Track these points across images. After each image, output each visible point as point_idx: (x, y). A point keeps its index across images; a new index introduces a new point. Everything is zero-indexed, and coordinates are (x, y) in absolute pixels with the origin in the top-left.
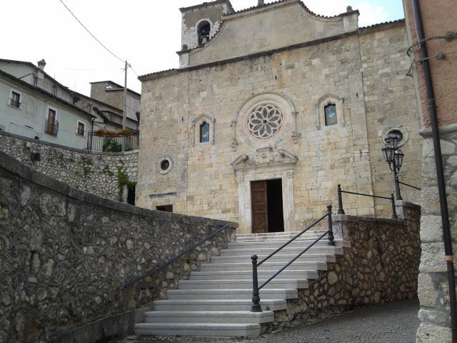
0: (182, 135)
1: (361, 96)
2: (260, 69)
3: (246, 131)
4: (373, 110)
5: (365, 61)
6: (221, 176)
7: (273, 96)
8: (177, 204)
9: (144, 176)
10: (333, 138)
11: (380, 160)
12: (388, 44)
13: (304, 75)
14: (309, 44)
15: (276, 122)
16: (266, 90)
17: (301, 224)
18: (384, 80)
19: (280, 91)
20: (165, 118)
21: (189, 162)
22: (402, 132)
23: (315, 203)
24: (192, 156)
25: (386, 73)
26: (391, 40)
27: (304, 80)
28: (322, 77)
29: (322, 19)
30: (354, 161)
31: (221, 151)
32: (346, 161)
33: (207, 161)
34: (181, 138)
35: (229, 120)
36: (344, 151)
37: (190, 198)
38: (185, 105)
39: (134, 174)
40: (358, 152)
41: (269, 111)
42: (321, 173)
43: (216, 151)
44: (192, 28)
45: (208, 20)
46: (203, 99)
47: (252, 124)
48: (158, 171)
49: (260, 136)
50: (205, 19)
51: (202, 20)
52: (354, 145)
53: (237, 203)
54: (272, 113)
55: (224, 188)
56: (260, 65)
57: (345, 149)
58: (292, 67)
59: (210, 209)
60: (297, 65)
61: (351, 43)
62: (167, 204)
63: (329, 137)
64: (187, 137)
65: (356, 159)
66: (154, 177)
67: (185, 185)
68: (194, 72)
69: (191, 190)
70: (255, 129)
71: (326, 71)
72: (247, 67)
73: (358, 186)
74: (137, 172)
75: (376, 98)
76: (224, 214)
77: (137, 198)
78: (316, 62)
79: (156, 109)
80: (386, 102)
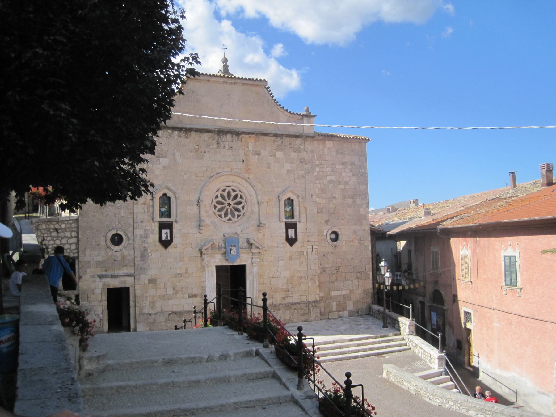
1: (314, 197)
2: (227, 147)
4: (322, 212)
5: (318, 166)
7: (239, 180)
9: (88, 250)
11: (324, 256)
12: (335, 154)
13: (269, 165)
14: (276, 135)
15: (240, 207)
18: (330, 186)
19: (246, 176)
22: (340, 233)
25: (332, 181)
26: (337, 151)
29: (285, 112)
32: (301, 254)
35: (194, 198)
37: (152, 281)
39: (73, 247)
40: (311, 247)
42: (281, 263)
46: (164, 167)
48: (108, 247)
52: (308, 241)
54: (236, 197)
55: (190, 271)
56: (227, 143)
58: (259, 154)
59: (176, 293)
61: (309, 146)
62: (123, 286)
64: (146, 210)
65: (309, 253)
66: (103, 253)
69: (152, 272)
70: (219, 210)
71: (288, 166)
72: (214, 142)
73: (309, 277)
74: (77, 244)
75: (324, 201)
76: (191, 299)
78: (279, 154)
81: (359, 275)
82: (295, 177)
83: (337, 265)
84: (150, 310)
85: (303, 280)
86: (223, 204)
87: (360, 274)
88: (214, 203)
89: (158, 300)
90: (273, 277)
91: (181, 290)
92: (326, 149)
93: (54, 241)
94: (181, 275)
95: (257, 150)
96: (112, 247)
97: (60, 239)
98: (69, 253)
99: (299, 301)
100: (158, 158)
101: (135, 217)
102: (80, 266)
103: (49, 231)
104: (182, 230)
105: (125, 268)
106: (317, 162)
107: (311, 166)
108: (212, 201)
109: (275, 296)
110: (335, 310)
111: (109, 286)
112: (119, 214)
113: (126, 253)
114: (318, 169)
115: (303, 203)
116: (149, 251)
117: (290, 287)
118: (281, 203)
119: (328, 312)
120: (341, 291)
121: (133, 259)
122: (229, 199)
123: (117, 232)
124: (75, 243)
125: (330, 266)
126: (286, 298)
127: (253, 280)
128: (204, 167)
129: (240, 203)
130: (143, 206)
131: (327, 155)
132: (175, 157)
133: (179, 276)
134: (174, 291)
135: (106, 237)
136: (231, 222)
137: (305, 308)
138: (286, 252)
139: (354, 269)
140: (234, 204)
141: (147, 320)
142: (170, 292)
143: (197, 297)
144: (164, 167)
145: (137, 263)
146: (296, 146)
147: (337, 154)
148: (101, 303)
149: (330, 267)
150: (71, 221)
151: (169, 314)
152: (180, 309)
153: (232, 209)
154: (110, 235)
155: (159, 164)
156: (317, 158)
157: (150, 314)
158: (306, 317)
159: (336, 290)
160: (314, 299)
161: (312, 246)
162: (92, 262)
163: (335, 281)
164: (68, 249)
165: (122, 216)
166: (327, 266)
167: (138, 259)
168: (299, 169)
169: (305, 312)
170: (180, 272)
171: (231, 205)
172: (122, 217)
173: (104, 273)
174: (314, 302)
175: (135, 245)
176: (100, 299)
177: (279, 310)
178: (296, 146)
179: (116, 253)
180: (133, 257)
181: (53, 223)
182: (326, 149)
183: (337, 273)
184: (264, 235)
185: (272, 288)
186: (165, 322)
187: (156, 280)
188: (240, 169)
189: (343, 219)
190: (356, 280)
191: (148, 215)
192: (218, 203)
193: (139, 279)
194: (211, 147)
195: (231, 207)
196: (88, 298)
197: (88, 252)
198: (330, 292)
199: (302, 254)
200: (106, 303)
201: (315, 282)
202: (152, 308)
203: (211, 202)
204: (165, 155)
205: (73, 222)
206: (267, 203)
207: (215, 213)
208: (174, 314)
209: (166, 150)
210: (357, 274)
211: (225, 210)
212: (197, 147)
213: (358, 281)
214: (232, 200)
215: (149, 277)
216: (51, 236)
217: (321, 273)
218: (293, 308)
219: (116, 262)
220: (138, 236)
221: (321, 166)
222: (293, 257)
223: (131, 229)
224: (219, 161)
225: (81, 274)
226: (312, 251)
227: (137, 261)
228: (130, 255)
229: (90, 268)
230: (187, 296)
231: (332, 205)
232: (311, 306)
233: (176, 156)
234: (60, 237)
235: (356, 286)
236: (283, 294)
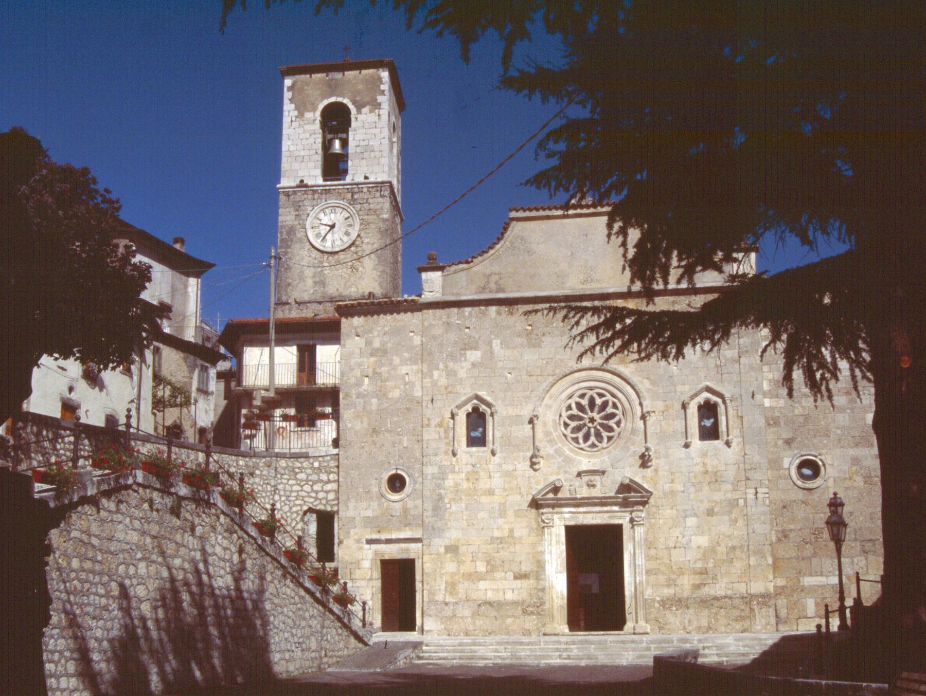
0: (432, 429)
1: (758, 397)
6: (510, 513)
8: (426, 558)
9: (353, 500)
10: (711, 463)
11: (784, 507)
17: (657, 605)
20: (396, 394)
21: (449, 482)
23: (681, 572)
24: (453, 472)
30: (746, 505)
32: (733, 504)
33: (484, 484)
34: (430, 434)
36: (729, 487)
37: (452, 549)
38: (436, 374)
39: (331, 496)
40: (753, 491)
41: (599, 401)
42: (691, 521)
43: (500, 465)
44: (309, 115)
45: (346, 101)
47: (568, 421)
49: (582, 445)
50: (340, 99)
51: (333, 99)
52: (747, 479)
53: (540, 565)
55: (517, 534)
57: (733, 484)
59: (492, 571)
62: (404, 556)
64: (443, 435)
65: (750, 502)
66: (375, 504)
67: (440, 524)
68: (455, 310)
69: (453, 535)
73: (751, 547)
76: (518, 582)
77: (341, 542)
79: (375, 373)
80: (796, 412)
81: (868, 546)
83: (816, 526)
84: (447, 597)
85: (738, 552)
86: (581, 418)
87: (870, 544)
89: (461, 580)
90: (675, 547)
91: (501, 565)
93: (302, 486)
94: (501, 540)
96: (389, 496)
97: (310, 483)
98: (325, 505)
99: (729, 592)
100: (463, 352)
101: (425, 446)
102: (340, 525)
103: (293, 471)
104: (504, 466)
105: (407, 528)
107: (750, 340)
108: (560, 416)
109: (678, 582)
110: (813, 615)
111: (383, 556)
112: (400, 443)
113: (410, 504)
115: (735, 408)
116: (446, 501)
117: (711, 565)
118: (688, 411)
119: (797, 617)
120: (827, 576)
121: (421, 513)
122: (592, 411)
124: (335, 491)
125: (799, 528)
126: (702, 586)
127: (635, 553)
128: (542, 359)
129: (612, 416)
130: (438, 429)
132: (491, 347)
133: (499, 541)
134: (489, 567)
136: (595, 449)
137: (743, 607)
139: (855, 534)
141: (441, 612)
142: (481, 567)
143: (529, 578)
144: (474, 365)
145: (427, 521)
148: (371, 584)
149: (800, 530)
150: (329, 458)
151: (479, 605)
152: (499, 597)
153: (598, 427)
154: (386, 476)
155: (465, 360)
157: (446, 604)
158: (746, 624)
159: (813, 574)
160: (763, 590)
161: (756, 489)
162: (358, 519)
163: (810, 558)
164: (323, 498)
165: (405, 445)
166: (792, 527)
167: (428, 513)
169: (743, 614)
170: (500, 535)
171: (595, 421)
173: (375, 536)
174: (763, 596)
175: (424, 491)
176: (368, 577)
177: (688, 608)
179: (394, 504)
180: (421, 510)
181: (299, 460)
183: (816, 541)
185: (674, 568)
186: (473, 616)
189: (828, 436)
190: (861, 555)
191: (446, 443)
192: (572, 417)
193: (430, 545)
194: (554, 325)
196: (351, 574)
197: (351, 505)
198: (801, 579)
199: (735, 503)
201: (764, 557)
202: (451, 593)
203: (558, 417)
204: (474, 345)
205: (332, 459)
206: (661, 413)
207: (565, 436)
208: (488, 606)
209: (477, 336)
210: (864, 544)
211: (585, 430)
212: (530, 328)
213: (866, 559)
214: (599, 413)
215: (447, 542)
216: (296, 479)
217: (779, 540)
218: (716, 605)
219: (394, 518)
220: (429, 477)
222: (716, 510)
223: (418, 466)
225: (341, 537)
226: (757, 498)
227: (427, 517)
228: (416, 507)
229: (355, 528)
230: (510, 575)
231: (801, 410)
232: (755, 603)
233: (494, 345)
234: (310, 480)
235: (862, 568)
236: (697, 580)
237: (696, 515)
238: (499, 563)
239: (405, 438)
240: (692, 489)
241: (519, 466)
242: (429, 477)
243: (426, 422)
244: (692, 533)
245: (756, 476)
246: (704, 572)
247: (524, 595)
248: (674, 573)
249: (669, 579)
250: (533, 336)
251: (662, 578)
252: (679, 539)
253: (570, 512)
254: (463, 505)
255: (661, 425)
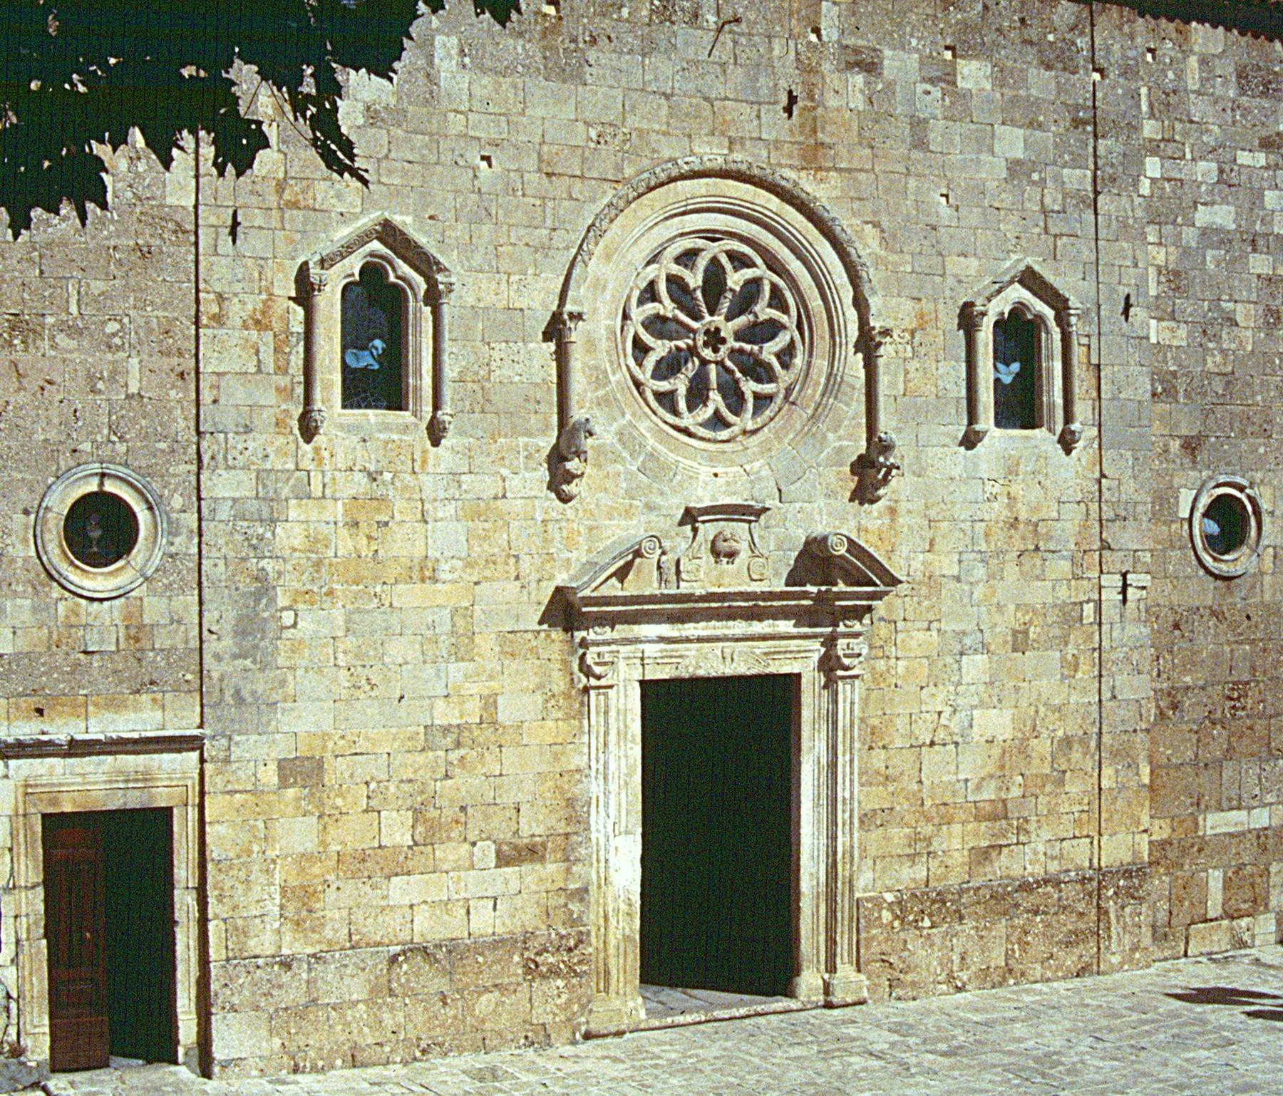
0: (232, 335)
3: (619, 378)
5: (1154, 148)
6: (486, 643)
10: (1027, 495)
11: (1176, 626)
13: (919, 125)
16: (740, 158)
17: (886, 916)
21: (289, 536)
25: (1219, 230)
27: (917, 154)
28: (992, 170)
31: (486, 485)
32: (1070, 616)
36: (1066, 565)
42: (975, 666)
52: (1105, 546)
55: (505, 715)
58: (871, 67)
60: (891, 60)
62: (134, 801)
63: (1016, 489)
64: (269, 363)
65: (1110, 612)
82: (1048, 201)
85: (1076, 755)
88: (636, 327)
89: (331, 877)
90: (932, 744)
92: (1193, 61)
94: (457, 735)
95: (860, 43)
96: (74, 576)
99: (1054, 867)
101: (206, 397)
106: (1150, 129)
108: (626, 316)
111: (54, 802)
113: (154, 609)
114: (1153, 167)
116: (282, 601)
117: (1016, 792)
120: (1250, 809)
121: (195, 644)
123: (101, 484)
125: (1201, 683)
126: (994, 854)
128: (588, 124)
130: (254, 334)
131: (1198, 93)
133: (449, 740)
135: (38, 512)
136: (724, 434)
137: (1081, 907)
138: (1000, 608)
140: (739, 336)
143: (542, 859)
146: (1051, 37)
147: (1242, 91)
151: (393, 960)
152: (452, 927)
154: (61, 501)
156: (1151, 106)
157: (287, 965)
159: (1225, 804)
161: (1124, 575)
165: (133, 389)
168: (1066, 157)
171: (723, 341)
172: (129, 397)
174: (1128, 874)
177: (961, 918)
178: (1051, 37)
182: (1193, 61)
184: (892, 511)
185: (928, 803)
187: (320, 764)
188: (777, 144)
193: (227, 761)
195: (723, 350)
200: (37, 901)
201: (1133, 765)
207: (638, 384)
211: (691, 368)
215: (284, 748)
217: (1162, 714)
220: (225, 512)
221: (1170, 149)
224: (667, 97)
226: (1124, 601)
227: (218, 658)
230: (487, 851)
232: (1111, 892)
233: (439, 53)
237: (985, 648)
238: (450, 813)
239: (134, 361)
240: (980, 572)
241: (514, 483)
242: (225, 512)
243: (210, 307)
244: (975, 701)
245: (1126, 538)
246: (998, 813)
247: (529, 918)
248: (929, 820)
249: (915, 838)
250: (562, 42)
251: (898, 834)
252: (943, 721)
253: (662, 639)
254: (338, 615)
255: (907, 373)
